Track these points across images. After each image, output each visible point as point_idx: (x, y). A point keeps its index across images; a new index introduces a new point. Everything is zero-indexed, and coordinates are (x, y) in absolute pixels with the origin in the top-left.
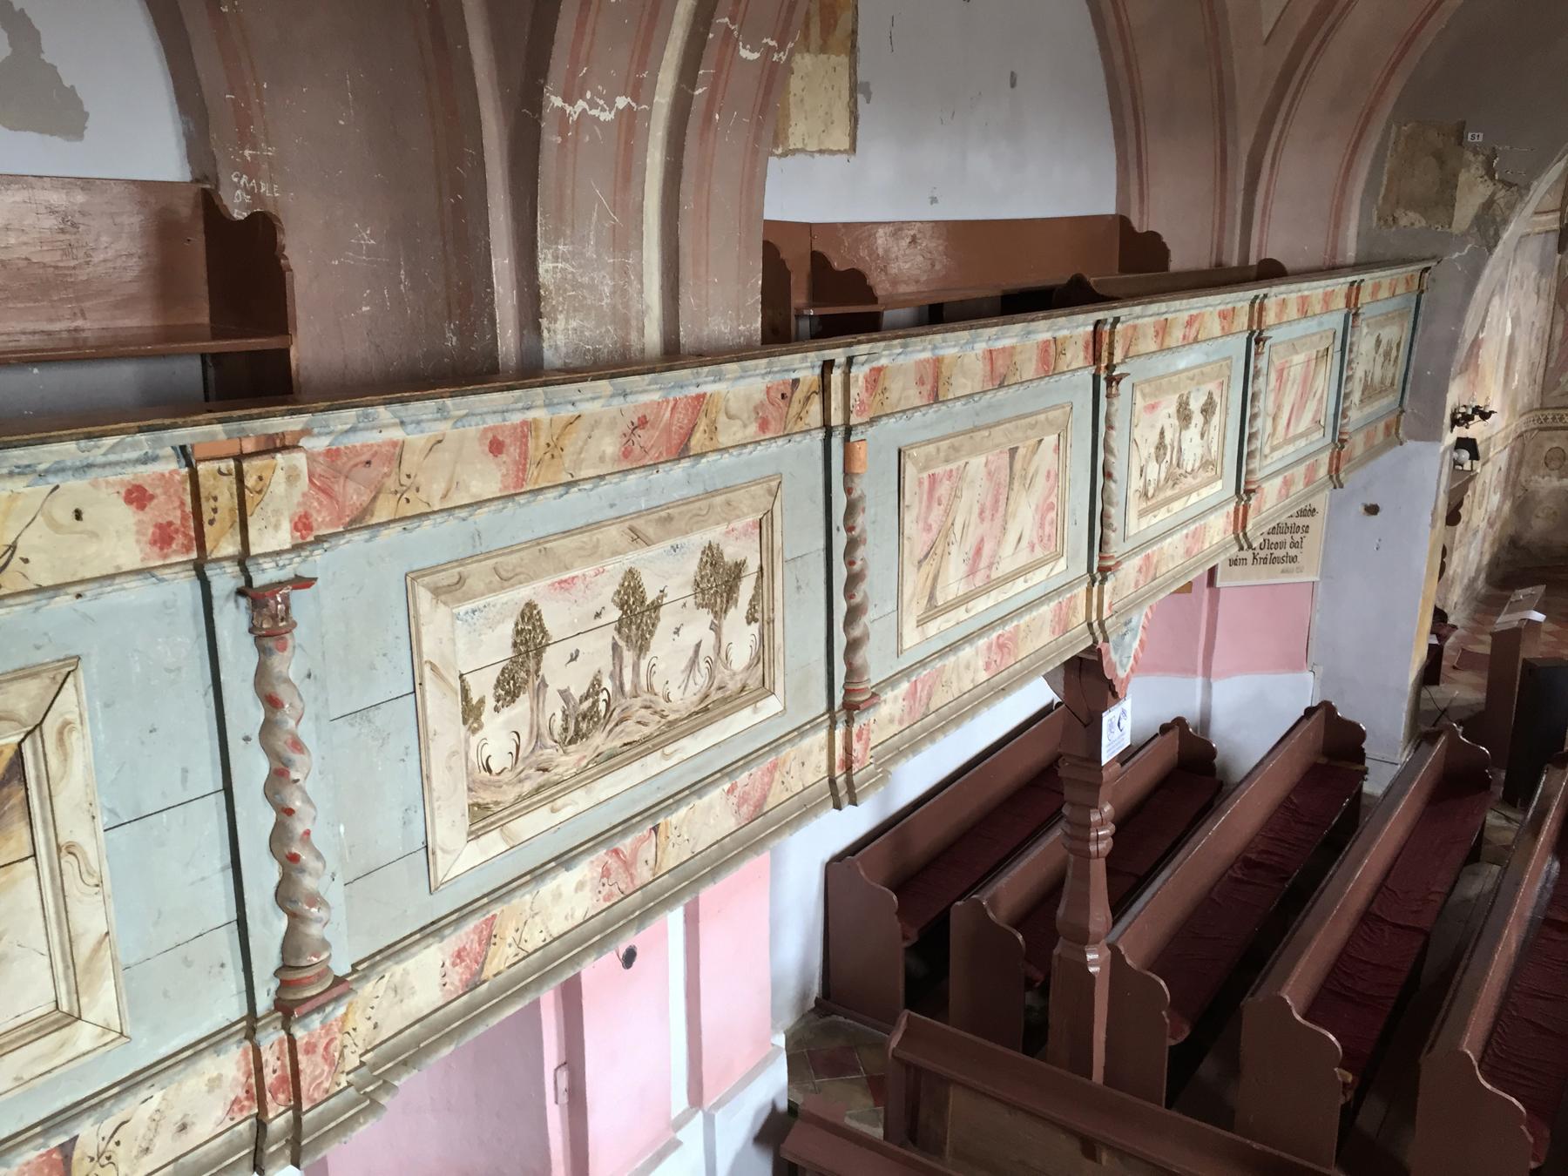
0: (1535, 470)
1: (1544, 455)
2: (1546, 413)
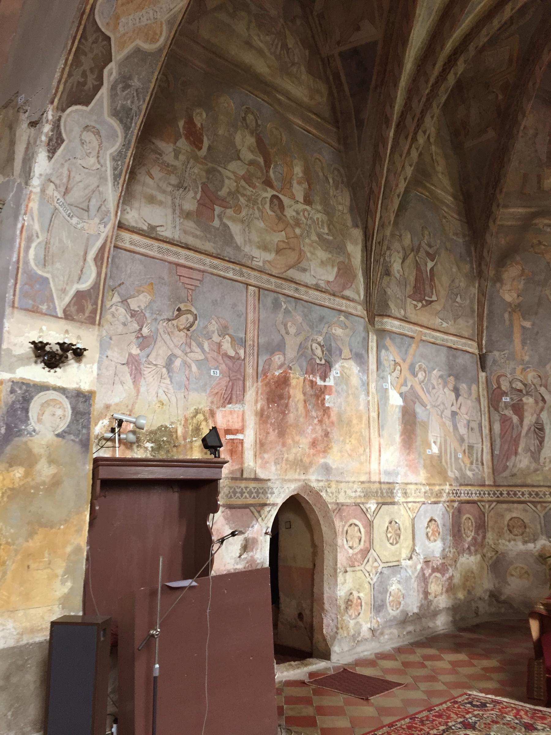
0: (500, 535)
1: (506, 523)
2: (501, 489)
